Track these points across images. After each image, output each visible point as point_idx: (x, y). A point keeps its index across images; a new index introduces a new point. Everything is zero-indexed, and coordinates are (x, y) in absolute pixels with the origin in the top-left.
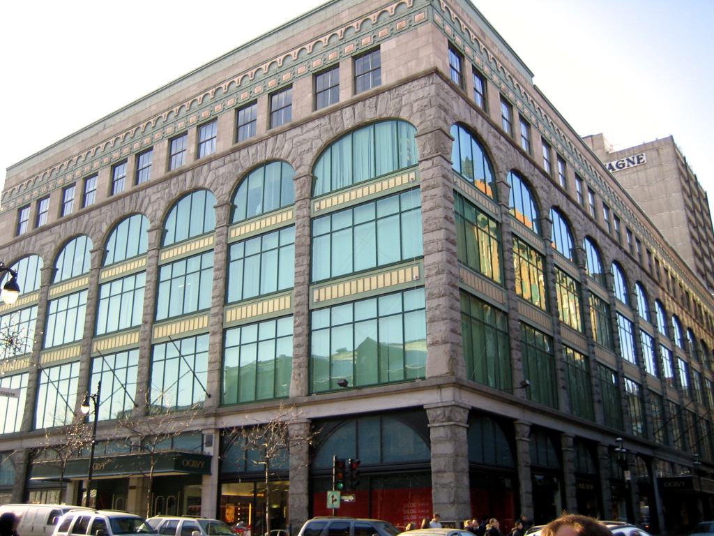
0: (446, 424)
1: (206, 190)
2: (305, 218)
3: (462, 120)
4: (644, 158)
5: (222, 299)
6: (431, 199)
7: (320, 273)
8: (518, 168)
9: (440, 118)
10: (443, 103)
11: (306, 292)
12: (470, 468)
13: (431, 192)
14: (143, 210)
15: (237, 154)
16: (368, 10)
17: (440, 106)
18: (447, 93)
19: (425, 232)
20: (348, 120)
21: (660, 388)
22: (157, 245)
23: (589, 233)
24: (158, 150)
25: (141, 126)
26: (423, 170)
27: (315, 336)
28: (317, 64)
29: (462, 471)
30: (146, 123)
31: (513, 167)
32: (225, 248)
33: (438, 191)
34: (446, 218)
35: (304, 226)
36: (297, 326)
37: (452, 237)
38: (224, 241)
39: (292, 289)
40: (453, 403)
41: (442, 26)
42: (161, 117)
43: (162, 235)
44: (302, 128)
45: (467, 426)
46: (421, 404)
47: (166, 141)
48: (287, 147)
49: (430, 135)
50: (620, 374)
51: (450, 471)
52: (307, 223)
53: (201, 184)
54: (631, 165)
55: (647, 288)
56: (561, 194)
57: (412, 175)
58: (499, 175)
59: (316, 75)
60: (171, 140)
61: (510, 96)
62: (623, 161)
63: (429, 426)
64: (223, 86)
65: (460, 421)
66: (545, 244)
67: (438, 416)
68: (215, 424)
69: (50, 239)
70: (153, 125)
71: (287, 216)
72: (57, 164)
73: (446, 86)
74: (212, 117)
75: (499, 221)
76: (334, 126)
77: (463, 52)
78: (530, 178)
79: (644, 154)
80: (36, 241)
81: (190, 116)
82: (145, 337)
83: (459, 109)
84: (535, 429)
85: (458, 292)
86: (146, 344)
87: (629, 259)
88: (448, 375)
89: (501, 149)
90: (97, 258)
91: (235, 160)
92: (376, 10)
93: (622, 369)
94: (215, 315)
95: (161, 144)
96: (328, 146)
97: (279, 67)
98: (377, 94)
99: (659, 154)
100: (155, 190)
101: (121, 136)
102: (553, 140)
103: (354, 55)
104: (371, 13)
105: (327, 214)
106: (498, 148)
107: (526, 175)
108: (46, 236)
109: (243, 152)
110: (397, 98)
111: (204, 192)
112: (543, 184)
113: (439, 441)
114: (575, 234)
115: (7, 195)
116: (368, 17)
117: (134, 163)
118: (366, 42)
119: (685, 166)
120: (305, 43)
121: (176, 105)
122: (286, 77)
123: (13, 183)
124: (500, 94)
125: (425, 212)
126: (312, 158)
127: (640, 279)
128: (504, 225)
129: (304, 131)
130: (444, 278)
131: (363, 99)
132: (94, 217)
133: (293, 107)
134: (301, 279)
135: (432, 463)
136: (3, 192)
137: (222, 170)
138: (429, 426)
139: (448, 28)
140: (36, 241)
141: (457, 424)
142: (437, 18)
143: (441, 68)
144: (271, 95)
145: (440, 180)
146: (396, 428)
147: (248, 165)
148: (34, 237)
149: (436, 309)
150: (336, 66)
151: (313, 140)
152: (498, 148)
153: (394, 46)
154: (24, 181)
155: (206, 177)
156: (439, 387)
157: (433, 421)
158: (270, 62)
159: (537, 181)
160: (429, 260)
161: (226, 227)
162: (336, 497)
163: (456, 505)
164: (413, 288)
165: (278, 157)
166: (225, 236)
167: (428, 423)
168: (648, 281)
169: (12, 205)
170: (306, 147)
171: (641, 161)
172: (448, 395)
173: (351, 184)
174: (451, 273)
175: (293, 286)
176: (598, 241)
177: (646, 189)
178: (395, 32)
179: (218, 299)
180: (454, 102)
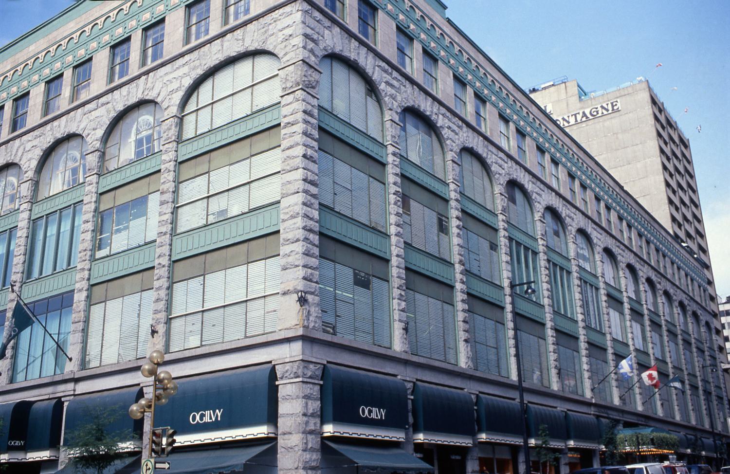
2: (171, 163)
4: (619, 105)
5: (89, 253)
6: (290, 136)
10: (309, 31)
11: (168, 242)
17: (306, 36)
18: (318, 21)
22: (29, 197)
24: (35, 93)
30: (24, 64)
34: (305, 156)
35: (169, 171)
37: (311, 177)
38: (94, 190)
48: (158, 86)
51: (296, 433)
54: (605, 112)
60: (48, 83)
62: (597, 108)
63: (277, 383)
65: (310, 377)
67: (287, 371)
68: (74, 390)
73: (317, 14)
76: (204, 63)
83: (333, 40)
85: (317, 237)
88: (298, 326)
89: (392, 86)
91: (108, 103)
106: (387, 83)
110: (263, 28)
112: (451, 125)
121: (53, 45)
125: (283, 151)
129: (175, 68)
131: (232, 30)
137: (94, 114)
138: (277, 383)
141: (305, 380)
147: (120, 107)
149: (289, 256)
151: (182, 77)
157: (282, 378)
170: (175, 85)
171: (615, 108)
172: (295, 350)
174: (308, 216)
177: (620, 136)
179: (85, 253)
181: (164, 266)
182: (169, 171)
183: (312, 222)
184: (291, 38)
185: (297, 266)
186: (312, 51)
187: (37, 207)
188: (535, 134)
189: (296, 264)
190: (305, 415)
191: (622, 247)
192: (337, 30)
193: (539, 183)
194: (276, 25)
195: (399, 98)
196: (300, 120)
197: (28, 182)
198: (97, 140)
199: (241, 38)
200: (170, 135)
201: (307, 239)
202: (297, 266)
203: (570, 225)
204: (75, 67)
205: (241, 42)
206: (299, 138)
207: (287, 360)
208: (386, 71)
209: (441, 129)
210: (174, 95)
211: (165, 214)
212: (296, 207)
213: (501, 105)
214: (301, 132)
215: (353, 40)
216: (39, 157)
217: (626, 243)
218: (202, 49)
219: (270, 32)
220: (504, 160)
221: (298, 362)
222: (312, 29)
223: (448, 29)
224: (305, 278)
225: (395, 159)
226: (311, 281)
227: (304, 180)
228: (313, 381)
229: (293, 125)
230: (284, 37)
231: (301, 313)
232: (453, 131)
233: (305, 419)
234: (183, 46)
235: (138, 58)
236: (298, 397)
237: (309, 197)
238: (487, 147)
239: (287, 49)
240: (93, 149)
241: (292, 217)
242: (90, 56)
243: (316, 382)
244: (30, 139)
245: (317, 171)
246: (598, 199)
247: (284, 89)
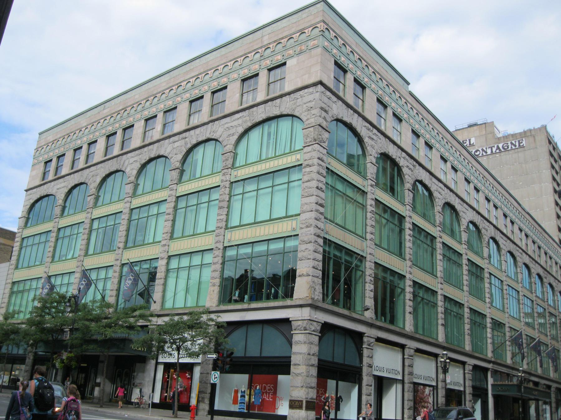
1: (166, 157)
2: (227, 182)
3: (339, 117)
4: (524, 142)
5: (170, 235)
6: (309, 174)
8: (387, 152)
9: (320, 116)
11: (223, 234)
12: (318, 364)
13: (308, 169)
14: (123, 169)
16: (281, 36)
17: (322, 108)
18: (329, 98)
19: (303, 196)
20: (260, 114)
22: (131, 194)
25: (128, 109)
26: (305, 153)
28: (246, 72)
29: (313, 365)
31: (382, 151)
32: (174, 200)
33: (315, 169)
34: (317, 188)
35: (226, 187)
36: (215, 257)
37: (321, 202)
39: (214, 231)
40: (309, 318)
41: (330, 50)
42: (141, 103)
45: (320, 335)
46: (288, 317)
47: (143, 121)
49: (312, 129)
51: (303, 365)
52: (228, 186)
53: (162, 153)
54: (514, 147)
55: (500, 243)
57: (298, 156)
59: (244, 80)
60: (147, 120)
61: (386, 99)
62: (508, 144)
63: (292, 332)
64: (182, 84)
65: (314, 331)
67: (299, 326)
69: (63, 185)
70: (135, 109)
72: (72, 133)
73: (328, 93)
74: (173, 106)
75: (366, 190)
76: (252, 118)
77: (347, 69)
79: (524, 139)
80: (54, 185)
81: (159, 104)
82: (117, 258)
86: (118, 263)
87: (484, 220)
88: (308, 298)
89: (373, 139)
90: (92, 200)
91: (186, 138)
92: (286, 37)
95: (140, 123)
96: (247, 131)
97: (220, 74)
98: (281, 96)
99: (535, 140)
101: (114, 115)
103: (268, 68)
104: (282, 38)
106: (370, 137)
107: (394, 157)
108: (61, 183)
109: (192, 132)
111: (165, 158)
113: (297, 343)
114: (436, 201)
115: (38, 152)
116: (280, 41)
117: (121, 135)
118: (279, 59)
120: (238, 58)
121: (151, 96)
122: (224, 81)
123: (43, 144)
126: (235, 140)
127: (493, 235)
128: (369, 194)
129: (232, 120)
130: (312, 230)
132: (92, 172)
133: (227, 102)
135: (292, 359)
136: (35, 150)
137: (177, 144)
138: (292, 332)
139: (335, 51)
140: (54, 185)
141: (311, 332)
142: (326, 43)
143: (325, 81)
144: (214, 93)
145: (316, 161)
146: (271, 332)
147: (194, 142)
148: (53, 183)
150: (257, 75)
153: (296, 63)
154: (50, 143)
155: (166, 148)
156: (301, 306)
158: (214, 70)
160: (303, 216)
162: (217, 376)
163: (304, 389)
164: (291, 236)
165: (213, 137)
166: (175, 191)
169: (41, 159)
170: (231, 131)
171: (521, 145)
172: (306, 313)
173: (273, 156)
174: (317, 227)
175: (215, 229)
178: (297, 53)
179: (167, 234)
181: (219, 249)
182: (226, 187)
183: (319, 230)
184: (312, 109)
185: (309, 259)
186: (325, 118)
187: (135, 200)
188: (464, 170)
189: (309, 257)
190: (309, 354)
191: (520, 251)
192: (340, 102)
193: (465, 205)
194: (302, 99)
195: (376, 147)
196: (316, 164)
197: (131, 184)
198: (177, 161)
199: (278, 105)
200: (227, 164)
201: (317, 242)
202: (309, 259)
203: (485, 235)
204: (165, 112)
205: (278, 108)
206: (316, 176)
207: (300, 319)
208: (369, 130)
209: (402, 168)
210: (231, 138)
211: (222, 215)
212: (310, 221)
213: (442, 150)
214: (316, 171)
215: (350, 110)
216: (138, 169)
217: (524, 248)
218: (251, 110)
219: (298, 104)
220: (442, 189)
221: (306, 321)
222: (325, 104)
223: (410, 99)
224: (314, 267)
225: (372, 189)
226: (317, 269)
227: (316, 203)
228: (315, 333)
229: (310, 166)
230: (306, 108)
231: (310, 290)
232: (410, 169)
233: (309, 357)
234: (238, 107)
235: (208, 110)
236: (305, 343)
237: (319, 215)
238: (431, 179)
239: (309, 117)
240: (175, 168)
241: (307, 227)
242: (175, 106)
243: (317, 334)
244: (133, 156)
245: (324, 198)
246: (505, 216)
247: (306, 143)
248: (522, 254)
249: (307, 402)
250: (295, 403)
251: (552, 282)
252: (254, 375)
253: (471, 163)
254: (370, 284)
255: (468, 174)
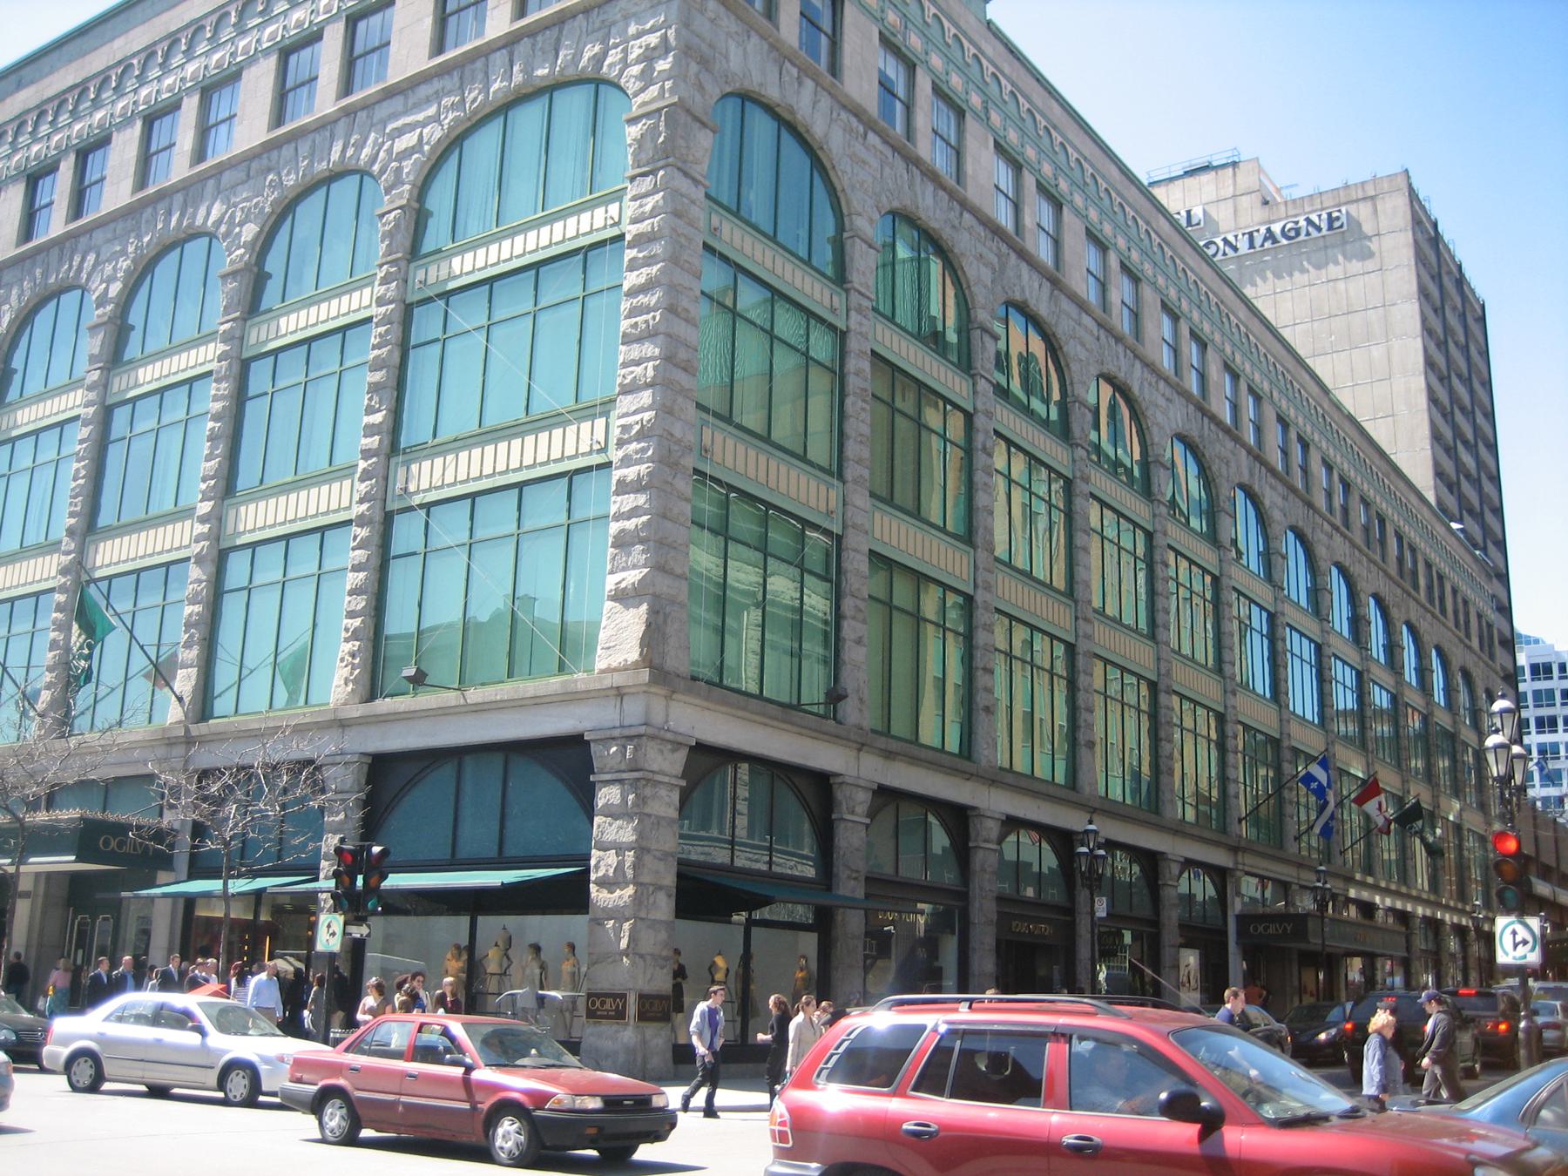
0: (624, 776)
7: (416, 429)
11: (381, 472)
15: (275, 154)
21: (1275, 724)
23: (1110, 368)
27: (396, 569)
31: (896, 204)
32: (236, 368)
43: (119, 334)
44: (406, 98)
50: (1162, 686)
55: (1267, 502)
56: (1035, 276)
58: (851, 220)
62: (1297, 223)
63: (592, 778)
66: (974, 385)
71: (360, 302)
75: (841, 325)
78: (946, 234)
79: (1344, 210)
84: (886, 795)
93: (1168, 673)
94: (203, 520)
95: (129, 131)
99: (1375, 211)
100: (109, 236)
102: (1030, 153)
105: (440, 296)
106: (854, 158)
107: (934, 225)
110: (600, 29)
119: (1436, 240)
124: (880, 33)
127: (1246, 479)
129: (410, 104)
133: (393, 48)
134: (373, 442)
141: (650, 776)
152: (854, 158)
159: (967, 243)
161: (240, 322)
167: (594, 773)
168: (1272, 487)
170: (409, 140)
171: (1337, 224)
176: (1136, 390)
180: (732, 46)
223: (991, 48)
248: (1331, 537)
249: (642, 997)
250: (603, 1003)
251: (1414, 620)
252: (480, 919)
253: (1182, 259)
254: (853, 623)
255: (1173, 293)
